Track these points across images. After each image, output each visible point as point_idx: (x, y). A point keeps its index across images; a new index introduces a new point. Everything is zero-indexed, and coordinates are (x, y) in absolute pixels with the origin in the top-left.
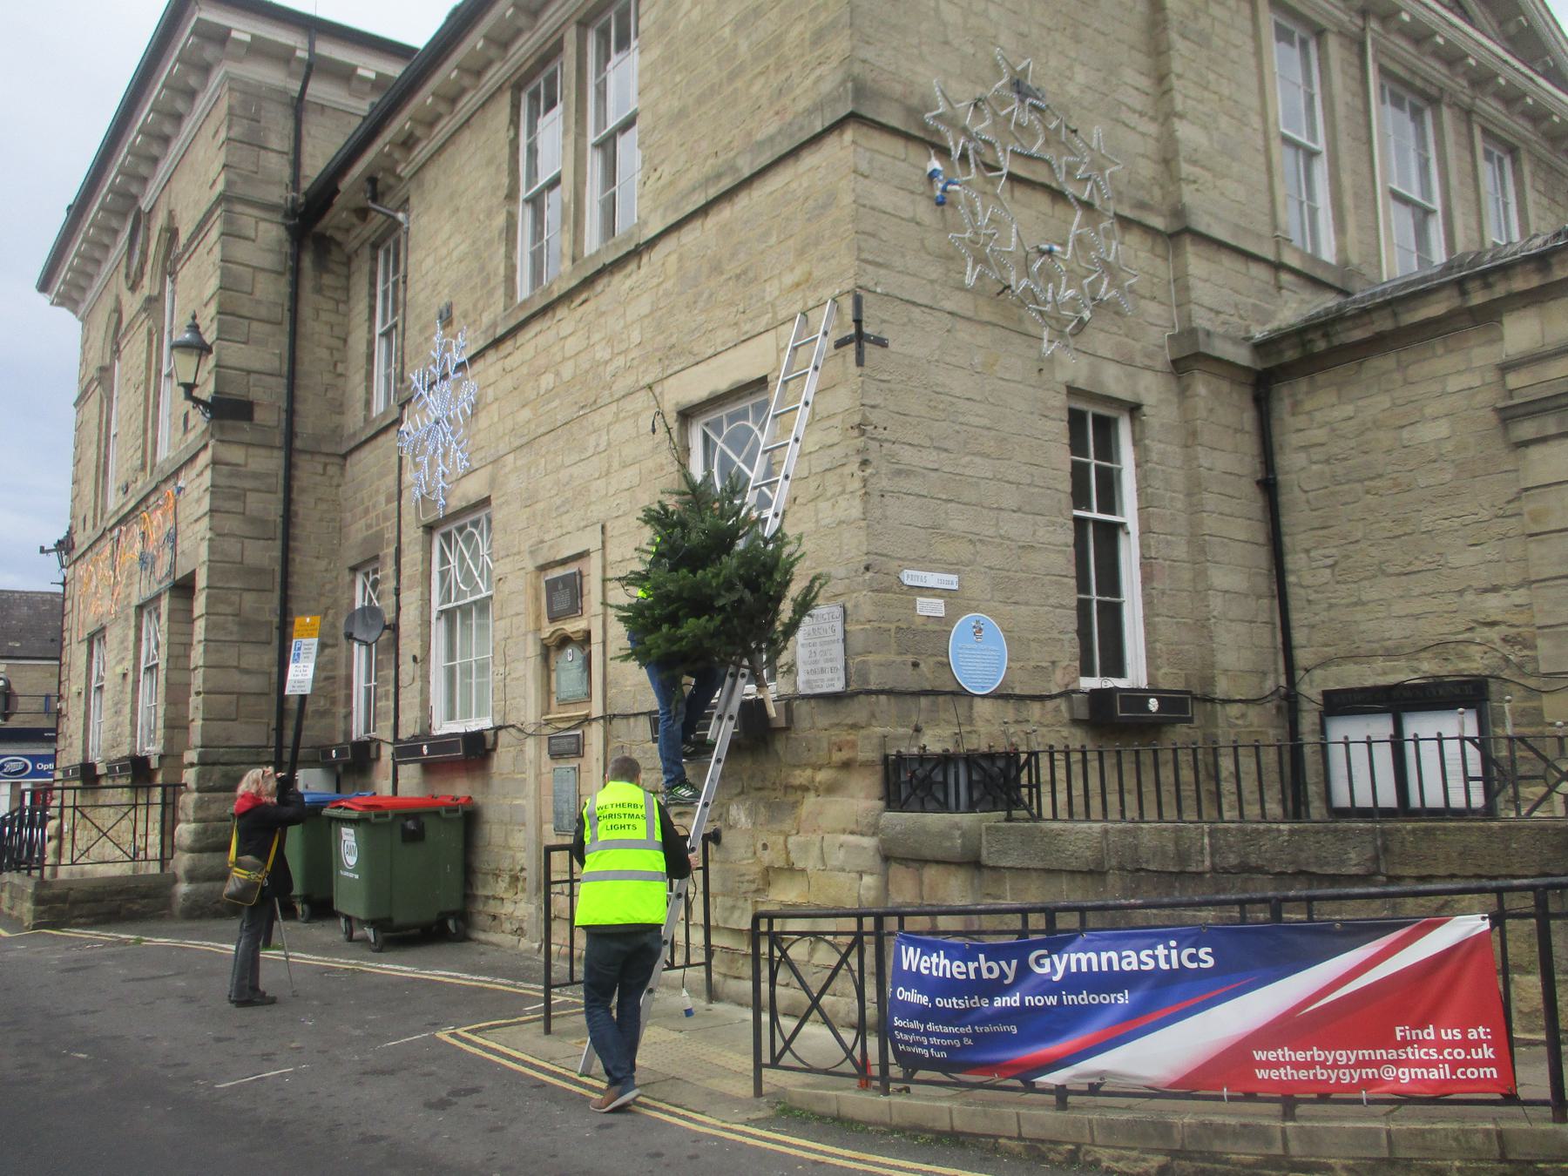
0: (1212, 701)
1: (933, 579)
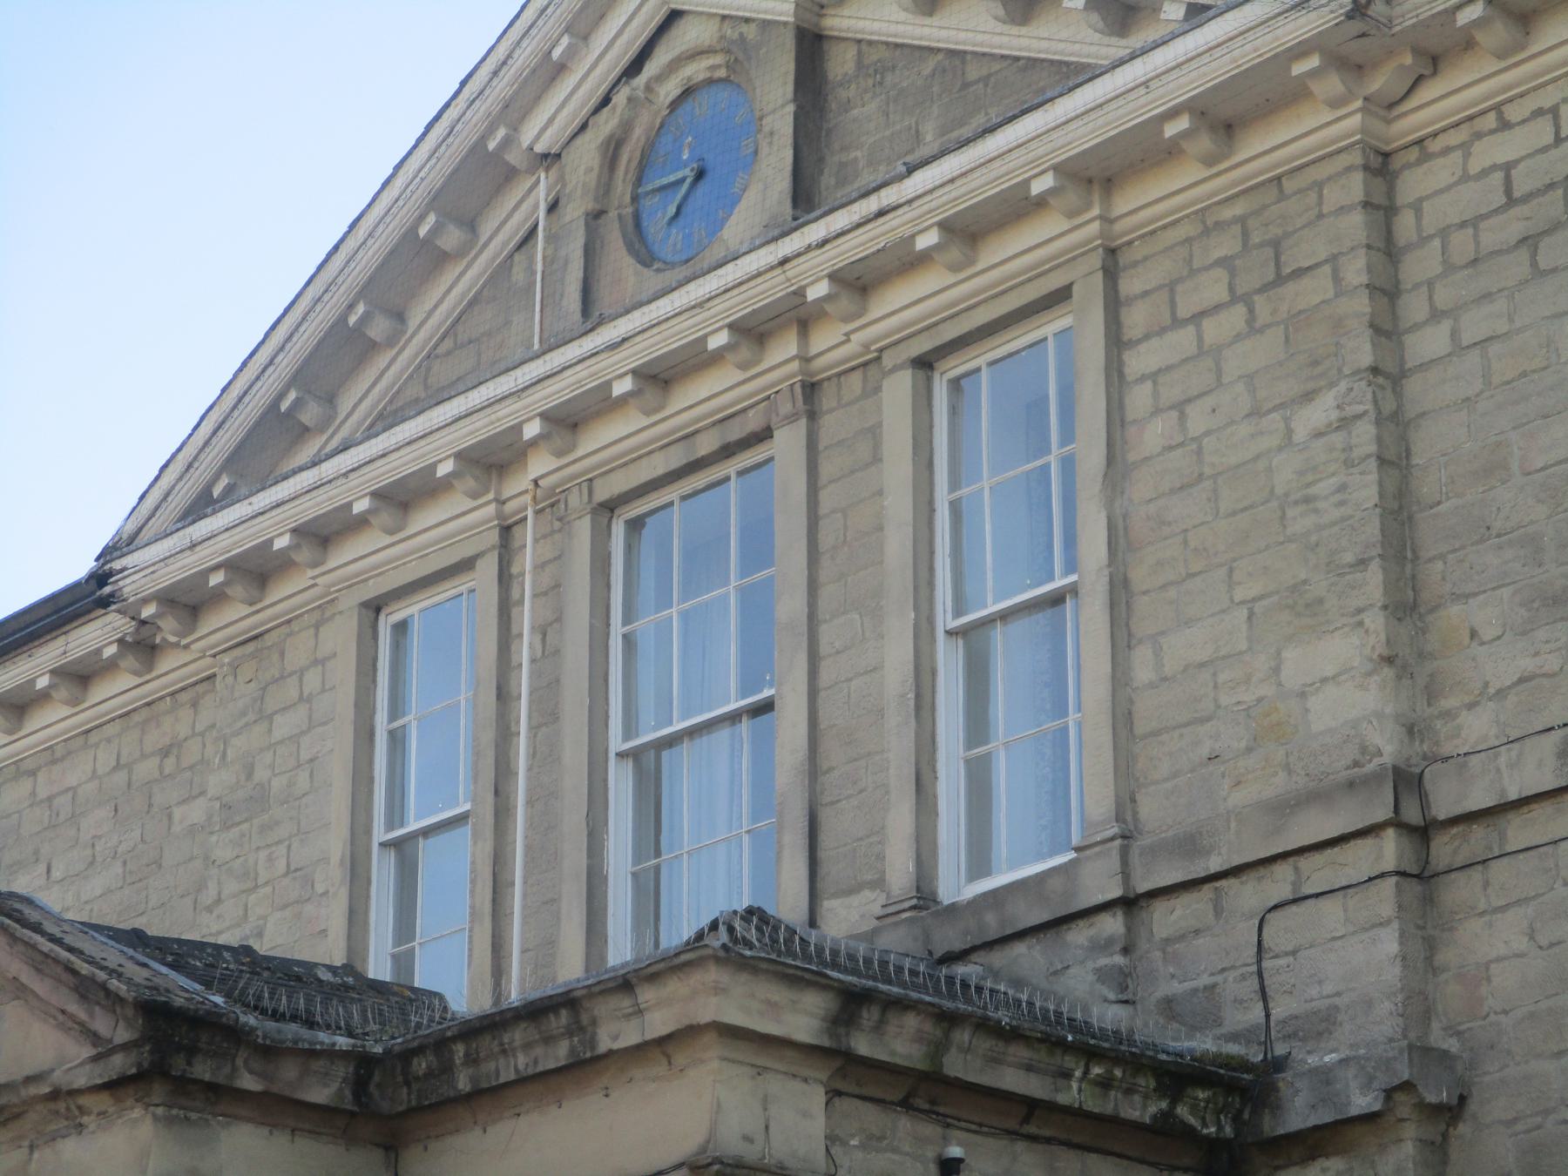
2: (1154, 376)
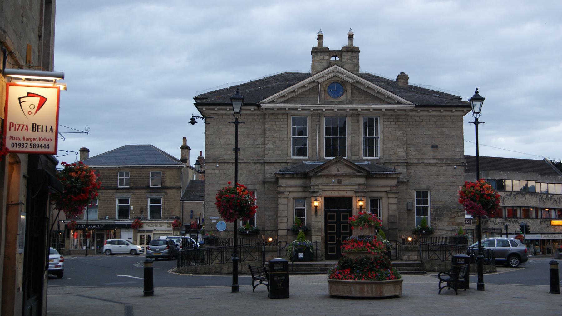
0: (264, 230)
1: (214, 218)
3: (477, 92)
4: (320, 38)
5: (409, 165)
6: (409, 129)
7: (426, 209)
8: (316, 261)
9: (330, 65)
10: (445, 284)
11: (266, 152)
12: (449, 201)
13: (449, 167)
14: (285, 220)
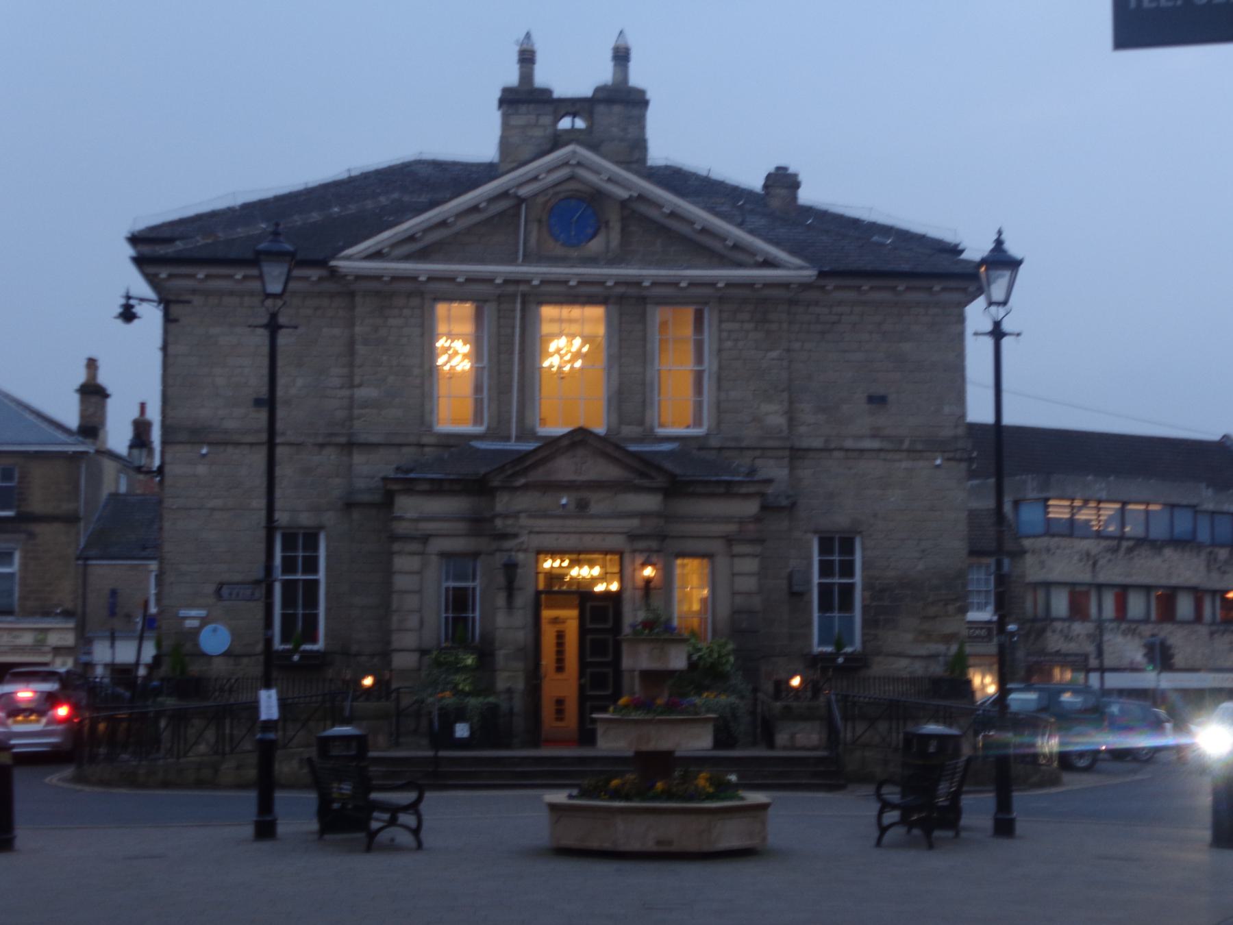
1: (193, 613)
2: (730, 331)
3: (999, 243)
4: (527, 58)
5: (796, 454)
6: (797, 345)
7: (848, 590)
8: (508, 746)
9: (558, 140)
10: (892, 816)
11: (356, 412)
12: (920, 566)
13: (921, 464)
14: (413, 622)
